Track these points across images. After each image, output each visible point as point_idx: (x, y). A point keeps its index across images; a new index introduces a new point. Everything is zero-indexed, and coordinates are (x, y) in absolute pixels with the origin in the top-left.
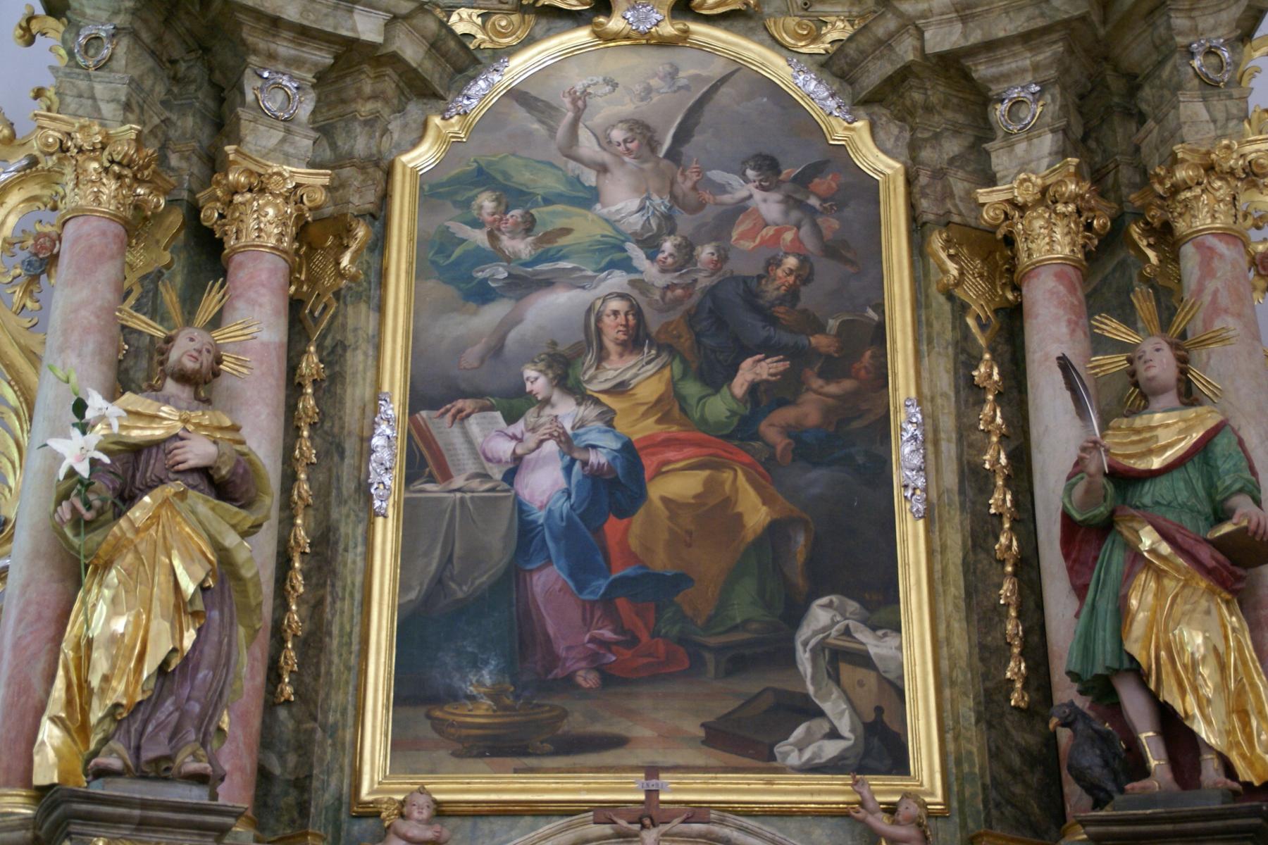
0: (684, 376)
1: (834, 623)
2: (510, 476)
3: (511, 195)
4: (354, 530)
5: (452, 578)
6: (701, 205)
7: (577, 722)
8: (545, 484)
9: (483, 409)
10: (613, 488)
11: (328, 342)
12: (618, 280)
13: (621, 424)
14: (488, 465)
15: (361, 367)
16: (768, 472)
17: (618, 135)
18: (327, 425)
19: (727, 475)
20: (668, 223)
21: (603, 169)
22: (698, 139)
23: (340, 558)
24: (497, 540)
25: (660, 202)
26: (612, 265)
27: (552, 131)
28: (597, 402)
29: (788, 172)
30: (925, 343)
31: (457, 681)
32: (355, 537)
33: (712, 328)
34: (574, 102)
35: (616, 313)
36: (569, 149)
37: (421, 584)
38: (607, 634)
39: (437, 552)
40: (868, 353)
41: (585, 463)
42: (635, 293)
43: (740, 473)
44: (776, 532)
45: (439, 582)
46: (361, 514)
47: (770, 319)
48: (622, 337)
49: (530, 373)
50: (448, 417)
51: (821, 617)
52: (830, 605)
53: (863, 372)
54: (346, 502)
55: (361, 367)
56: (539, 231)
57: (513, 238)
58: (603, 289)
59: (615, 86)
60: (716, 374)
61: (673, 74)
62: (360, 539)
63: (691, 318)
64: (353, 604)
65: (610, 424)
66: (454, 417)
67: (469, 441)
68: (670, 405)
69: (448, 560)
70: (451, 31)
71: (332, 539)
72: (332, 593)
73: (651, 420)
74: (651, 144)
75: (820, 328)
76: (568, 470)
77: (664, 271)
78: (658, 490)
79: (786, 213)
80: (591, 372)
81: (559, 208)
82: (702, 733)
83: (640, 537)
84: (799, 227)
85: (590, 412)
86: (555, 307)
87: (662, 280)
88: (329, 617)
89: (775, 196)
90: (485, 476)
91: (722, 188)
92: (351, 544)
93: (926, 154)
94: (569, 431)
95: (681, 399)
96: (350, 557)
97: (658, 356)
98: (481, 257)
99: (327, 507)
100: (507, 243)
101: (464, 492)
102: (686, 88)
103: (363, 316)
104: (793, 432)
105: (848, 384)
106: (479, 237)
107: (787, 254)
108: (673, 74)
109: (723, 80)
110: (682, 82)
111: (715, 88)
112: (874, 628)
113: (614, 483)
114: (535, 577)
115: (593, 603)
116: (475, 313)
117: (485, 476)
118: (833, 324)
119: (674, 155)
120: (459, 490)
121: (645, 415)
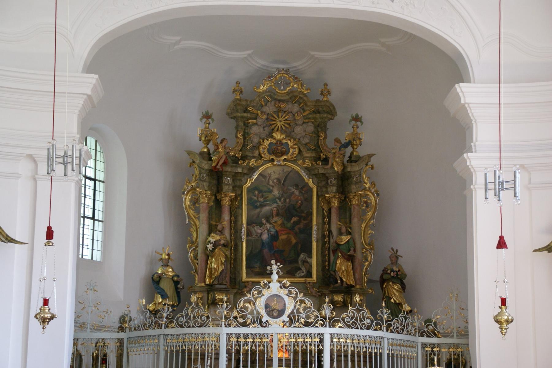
2: (261, 236)
3: (260, 191)
8: (265, 237)
10: (274, 237)
12: (275, 205)
13: (276, 228)
17: (275, 181)
20: (282, 196)
21: (273, 187)
26: (274, 203)
29: (300, 187)
44: (296, 244)
56: (264, 197)
58: (273, 206)
60: (289, 219)
68: (282, 225)
69: (252, 248)
74: (280, 183)
75: (303, 212)
85: (271, 226)
86: (267, 209)
87: (281, 205)
90: (257, 236)
98: (256, 201)
106: (256, 198)
108: (283, 171)
109: (291, 171)
117: (257, 236)
118: (305, 212)
119: (283, 184)
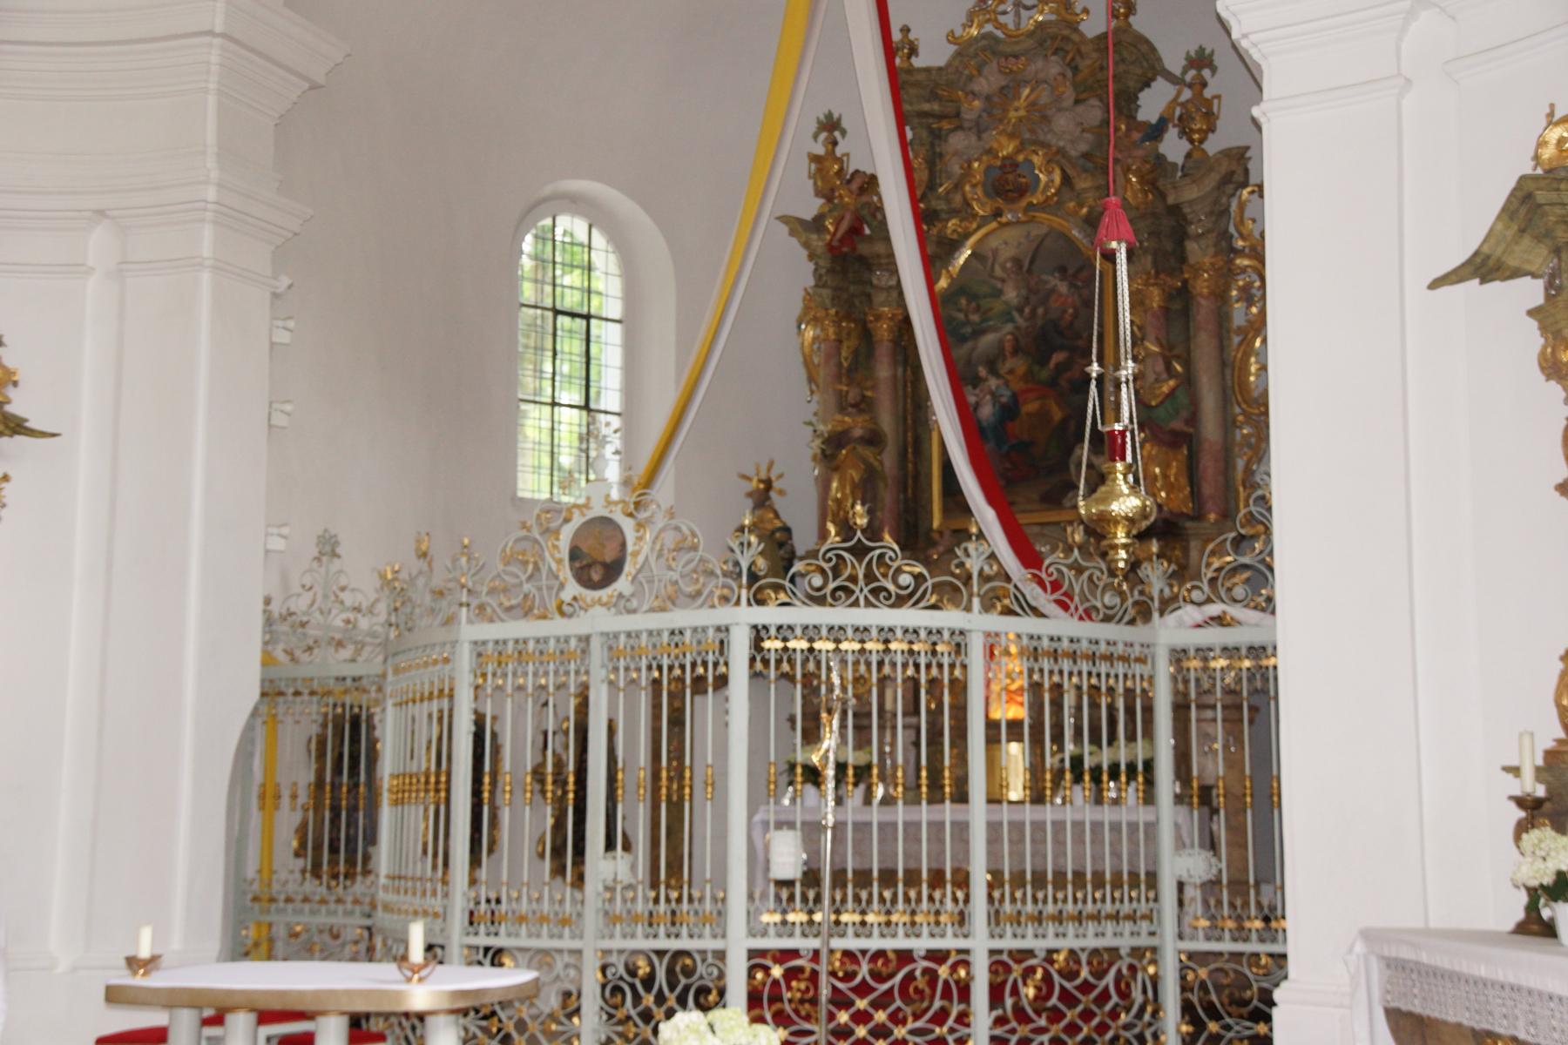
3: (973, 297)
12: (1009, 327)
20: (1027, 299)
21: (1003, 281)
29: (1071, 271)
36: (991, 275)
60: (1043, 361)
68: (1029, 376)
85: (1000, 382)
91: (1046, 282)
106: (961, 316)
109: (1046, 235)
119: (1029, 271)
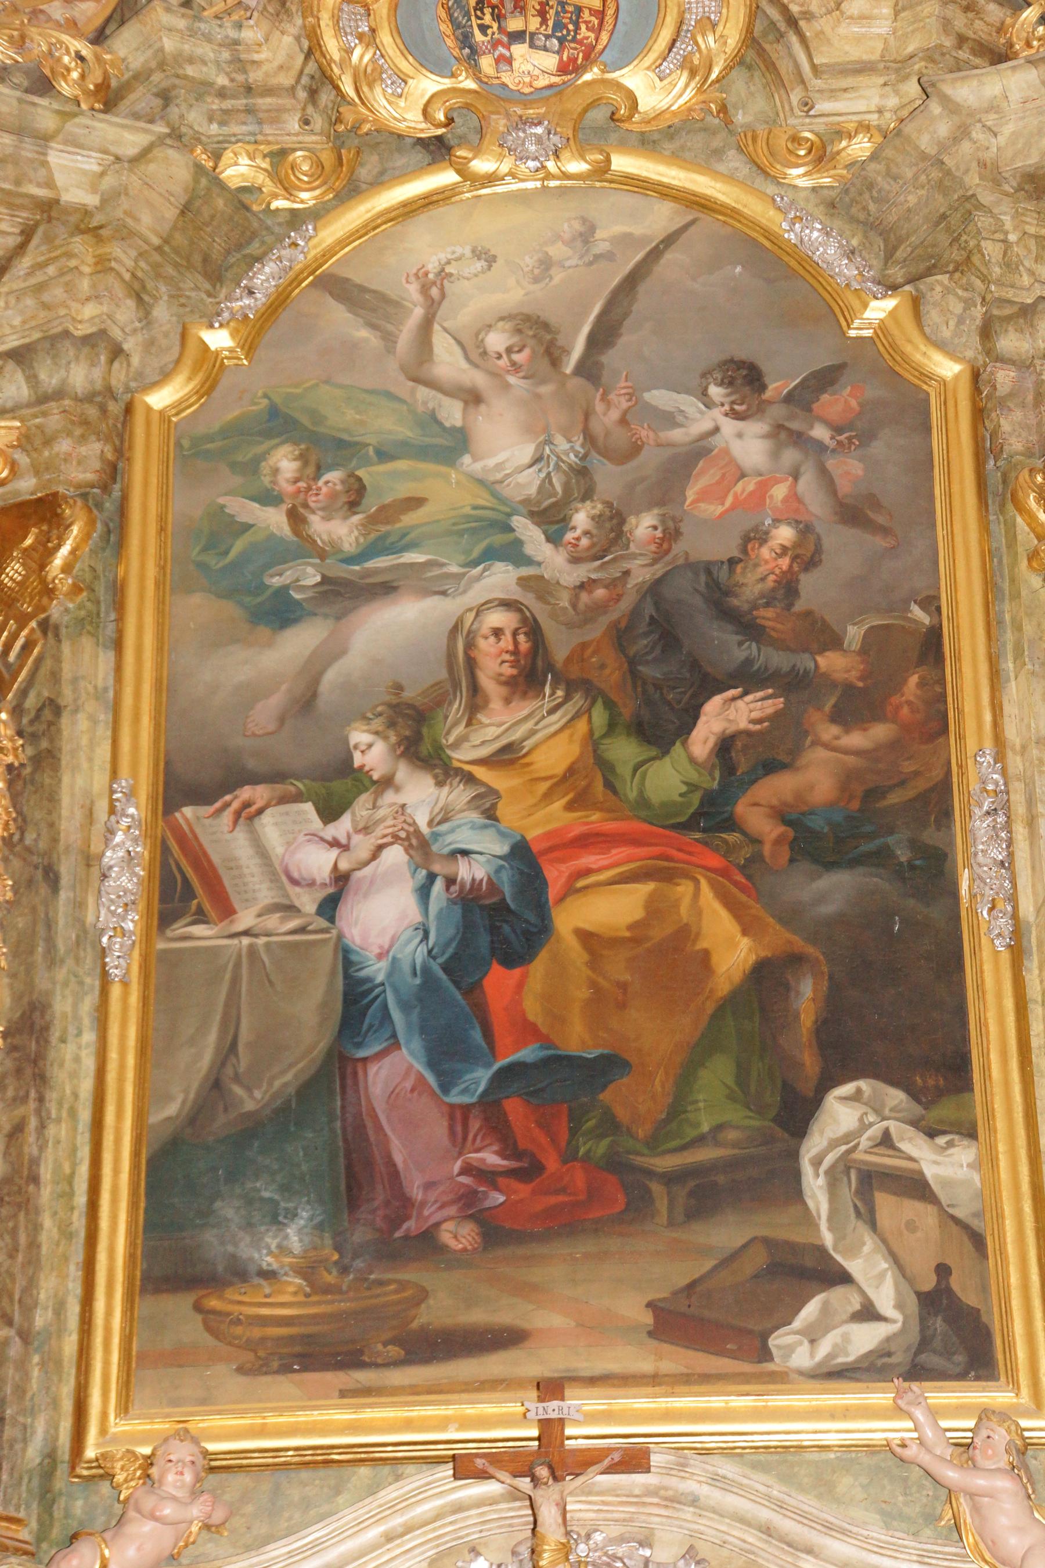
0: (612, 727)
1: (864, 1127)
2: (329, 907)
3: (324, 449)
4: (75, 1006)
5: (237, 1078)
6: (636, 449)
7: (444, 1306)
9: (284, 800)
10: (498, 922)
11: (31, 702)
12: (501, 579)
14: (293, 891)
15: (84, 741)
16: (746, 882)
17: (497, 341)
18: (30, 838)
19: (684, 889)
21: (473, 398)
22: (627, 339)
23: (52, 1054)
24: (309, 1015)
25: (567, 448)
26: (490, 555)
27: (389, 339)
28: (470, 779)
29: (776, 387)
30: (1010, 657)
31: (245, 1250)
32: (76, 1017)
33: (654, 652)
34: (425, 290)
35: (497, 632)
36: (419, 369)
37: (186, 1092)
38: (491, 1158)
39: (212, 1037)
40: (914, 680)
41: (450, 881)
42: (529, 600)
43: (704, 884)
44: (768, 978)
45: (216, 1084)
46: (88, 980)
47: (749, 628)
48: (508, 670)
49: (359, 736)
50: (227, 816)
51: (845, 1116)
52: (857, 1097)
53: (905, 710)
54: (62, 961)
55: (84, 741)
56: (371, 504)
57: (327, 519)
58: (476, 595)
59: (491, 260)
60: (661, 726)
61: (587, 235)
62: (86, 1022)
63: (621, 635)
64: (75, 1129)
65: (491, 814)
66: (238, 814)
67: (262, 852)
68: (589, 781)
69: (229, 1049)
70: (220, 184)
71: (39, 1022)
72: (38, 1112)
73: (559, 805)
74: (553, 354)
75: (834, 642)
76: (424, 892)
77: (575, 560)
78: (569, 919)
79: (775, 455)
80: (460, 729)
81: (402, 465)
82: (648, 1319)
83: (542, 998)
84: (796, 476)
85: (459, 795)
86: (397, 630)
87: (572, 575)
88: (35, 1151)
89: (756, 428)
91: (670, 419)
92: (72, 1030)
93: (1009, 342)
94: (425, 829)
95: (606, 767)
96: (69, 1050)
97: (567, 698)
98: (279, 554)
99: (30, 968)
100: (320, 527)
101: (256, 936)
102: (609, 256)
103: (86, 657)
104: (791, 817)
105: (880, 732)
106: (274, 520)
107: (777, 521)
108: (587, 235)
109: (669, 241)
110: (602, 247)
111: (655, 254)
112: (932, 1134)
113: (501, 909)
114: (373, 1069)
115: (466, 1109)
116: (270, 644)
117: (290, 909)
118: (854, 634)
119: (589, 370)
120: (246, 933)
121: (548, 797)
